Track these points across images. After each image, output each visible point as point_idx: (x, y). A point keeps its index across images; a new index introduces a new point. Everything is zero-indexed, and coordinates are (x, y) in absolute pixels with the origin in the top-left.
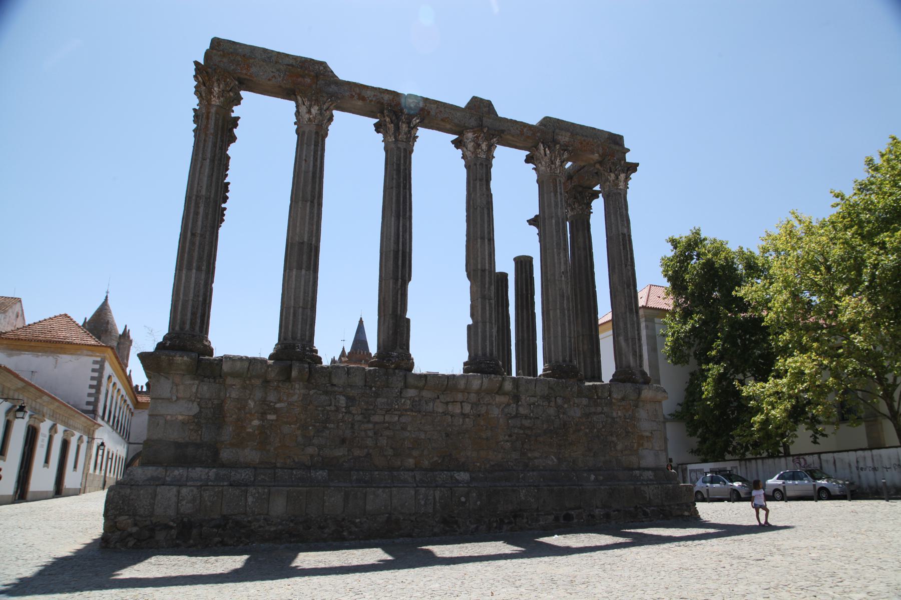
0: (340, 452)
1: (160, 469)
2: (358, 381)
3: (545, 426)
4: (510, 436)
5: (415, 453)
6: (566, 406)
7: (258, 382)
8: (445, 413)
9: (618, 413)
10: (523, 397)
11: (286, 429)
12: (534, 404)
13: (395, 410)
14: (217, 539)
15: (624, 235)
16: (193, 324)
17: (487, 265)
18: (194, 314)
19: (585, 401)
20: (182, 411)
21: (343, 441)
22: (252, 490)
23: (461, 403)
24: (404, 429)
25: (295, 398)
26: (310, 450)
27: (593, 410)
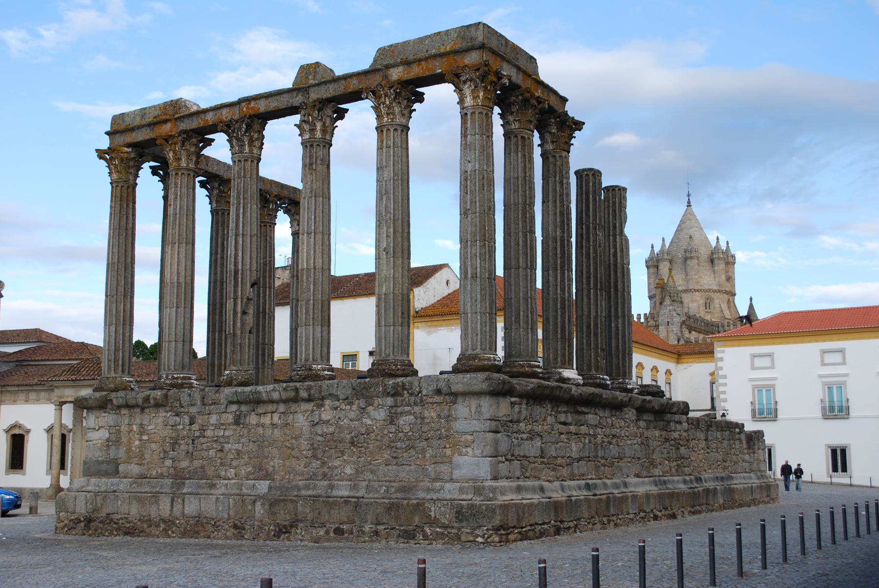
0: (184, 464)
4: (312, 445)
5: (234, 463)
6: (370, 408)
7: (138, 410)
8: (258, 425)
9: (430, 414)
10: (327, 402)
11: (153, 446)
12: (336, 409)
13: (222, 424)
14: (99, 531)
17: (305, 264)
19: (389, 401)
24: (228, 443)
26: (168, 463)
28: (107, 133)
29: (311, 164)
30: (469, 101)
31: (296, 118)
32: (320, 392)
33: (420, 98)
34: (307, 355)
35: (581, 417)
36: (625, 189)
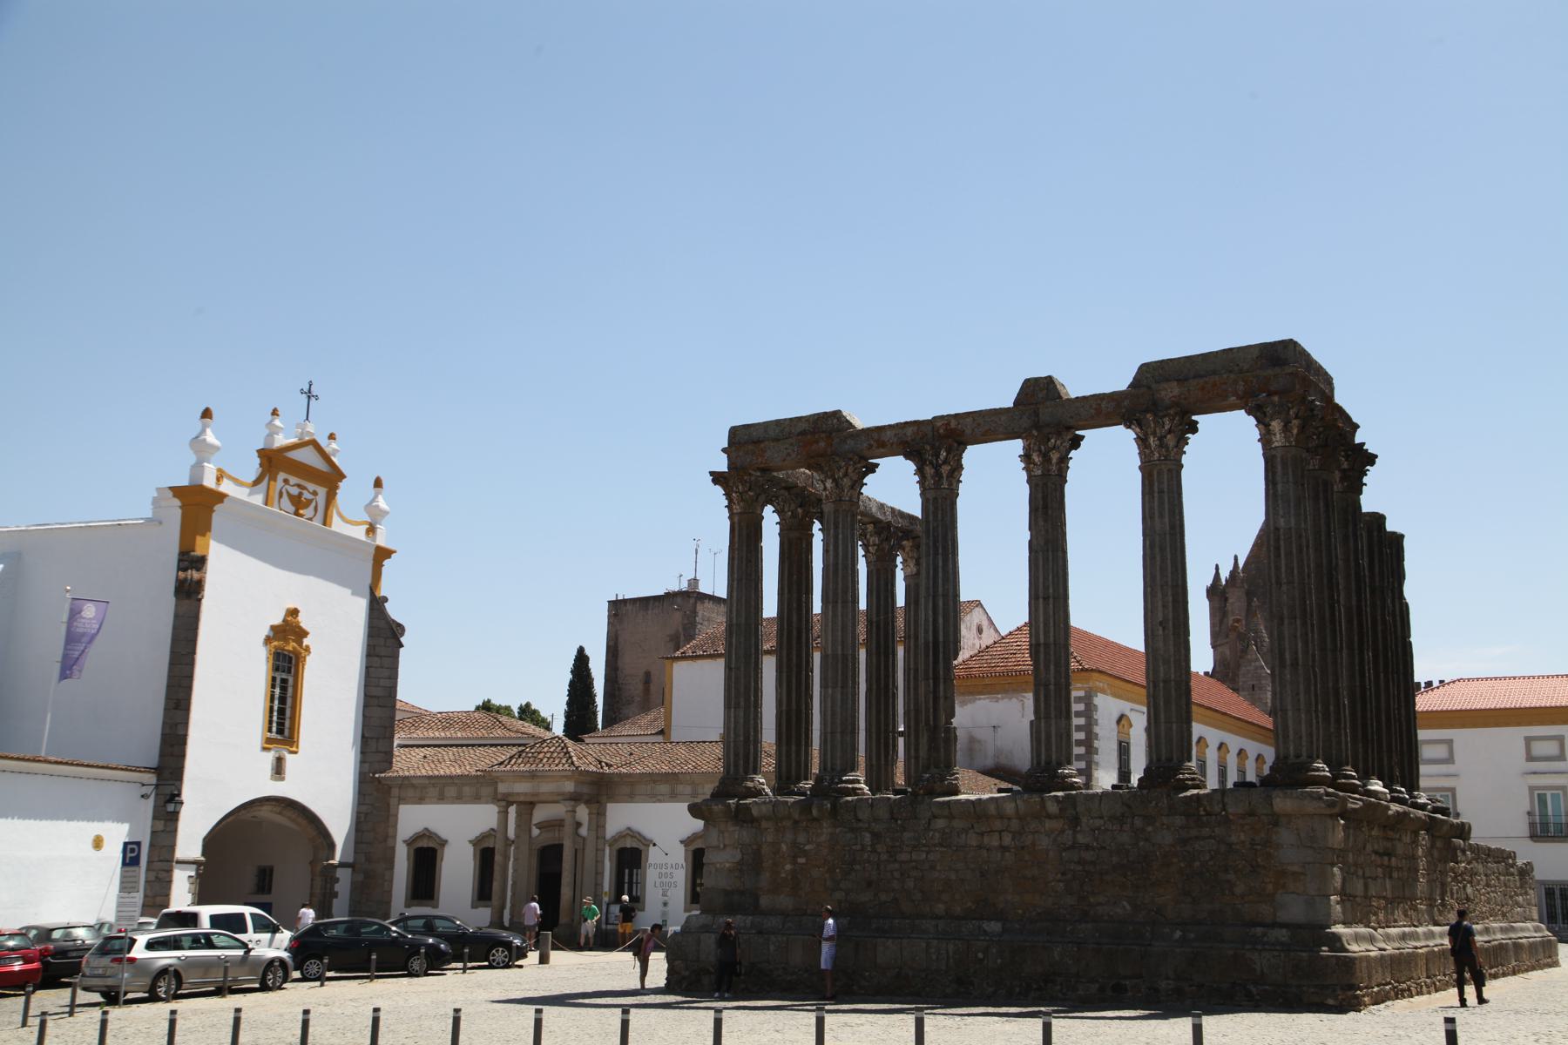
1: (710, 917)
2: (883, 813)
3: (1115, 859)
4: (1063, 874)
6: (1150, 829)
7: (788, 823)
8: (980, 847)
10: (1084, 820)
15: (1277, 529)
16: (736, 766)
18: (736, 755)
19: (1179, 821)
20: (722, 859)
21: (869, 884)
22: (773, 938)
23: (1000, 832)
24: (933, 868)
25: (823, 838)
26: (839, 895)
27: (1194, 833)
28: (724, 450)
29: (1045, 507)
30: (1278, 440)
31: (1016, 446)
32: (1074, 806)
33: (1193, 428)
34: (1049, 756)
35: (1389, 845)
36: (1402, 536)
